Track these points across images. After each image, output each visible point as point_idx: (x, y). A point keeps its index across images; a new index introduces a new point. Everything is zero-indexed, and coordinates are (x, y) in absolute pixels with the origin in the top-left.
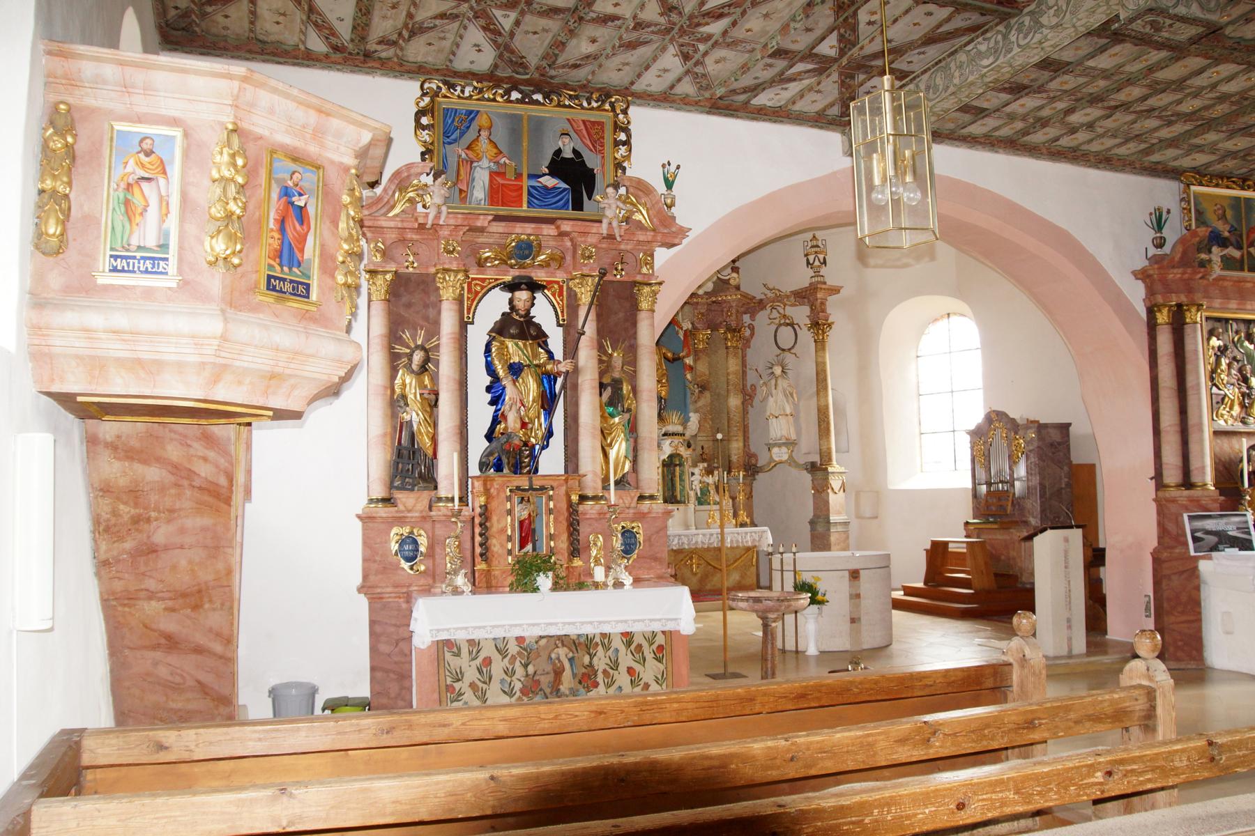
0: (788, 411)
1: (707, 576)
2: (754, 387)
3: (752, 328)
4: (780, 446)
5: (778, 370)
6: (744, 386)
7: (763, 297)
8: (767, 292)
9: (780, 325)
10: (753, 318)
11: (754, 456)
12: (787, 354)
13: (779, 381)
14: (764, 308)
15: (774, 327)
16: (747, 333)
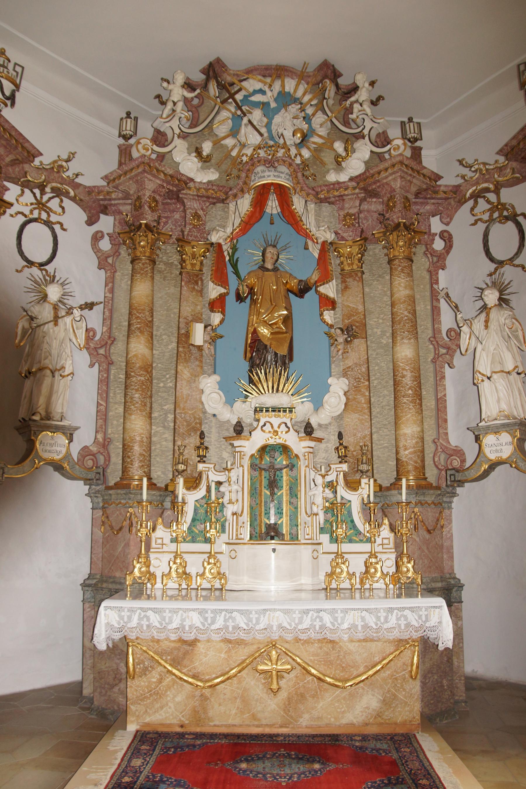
0: (510, 367)
1: (302, 697)
2: (455, 334)
3: (447, 238)
4: (496, 430)
5: (491, 297)
6: (436, 331)
7: (460, 181)
8: (466, 171)
9: (491, 220)
10: (447, 220)
11: (459, 453)
12: (507, 269)
13: (493, 314)
14: (462, 202)
15: (482, 226)
16: (439, 245)
